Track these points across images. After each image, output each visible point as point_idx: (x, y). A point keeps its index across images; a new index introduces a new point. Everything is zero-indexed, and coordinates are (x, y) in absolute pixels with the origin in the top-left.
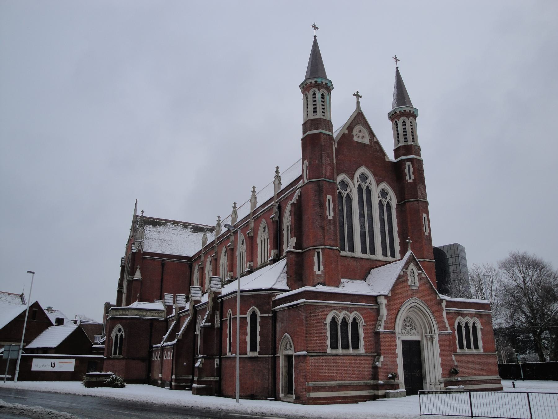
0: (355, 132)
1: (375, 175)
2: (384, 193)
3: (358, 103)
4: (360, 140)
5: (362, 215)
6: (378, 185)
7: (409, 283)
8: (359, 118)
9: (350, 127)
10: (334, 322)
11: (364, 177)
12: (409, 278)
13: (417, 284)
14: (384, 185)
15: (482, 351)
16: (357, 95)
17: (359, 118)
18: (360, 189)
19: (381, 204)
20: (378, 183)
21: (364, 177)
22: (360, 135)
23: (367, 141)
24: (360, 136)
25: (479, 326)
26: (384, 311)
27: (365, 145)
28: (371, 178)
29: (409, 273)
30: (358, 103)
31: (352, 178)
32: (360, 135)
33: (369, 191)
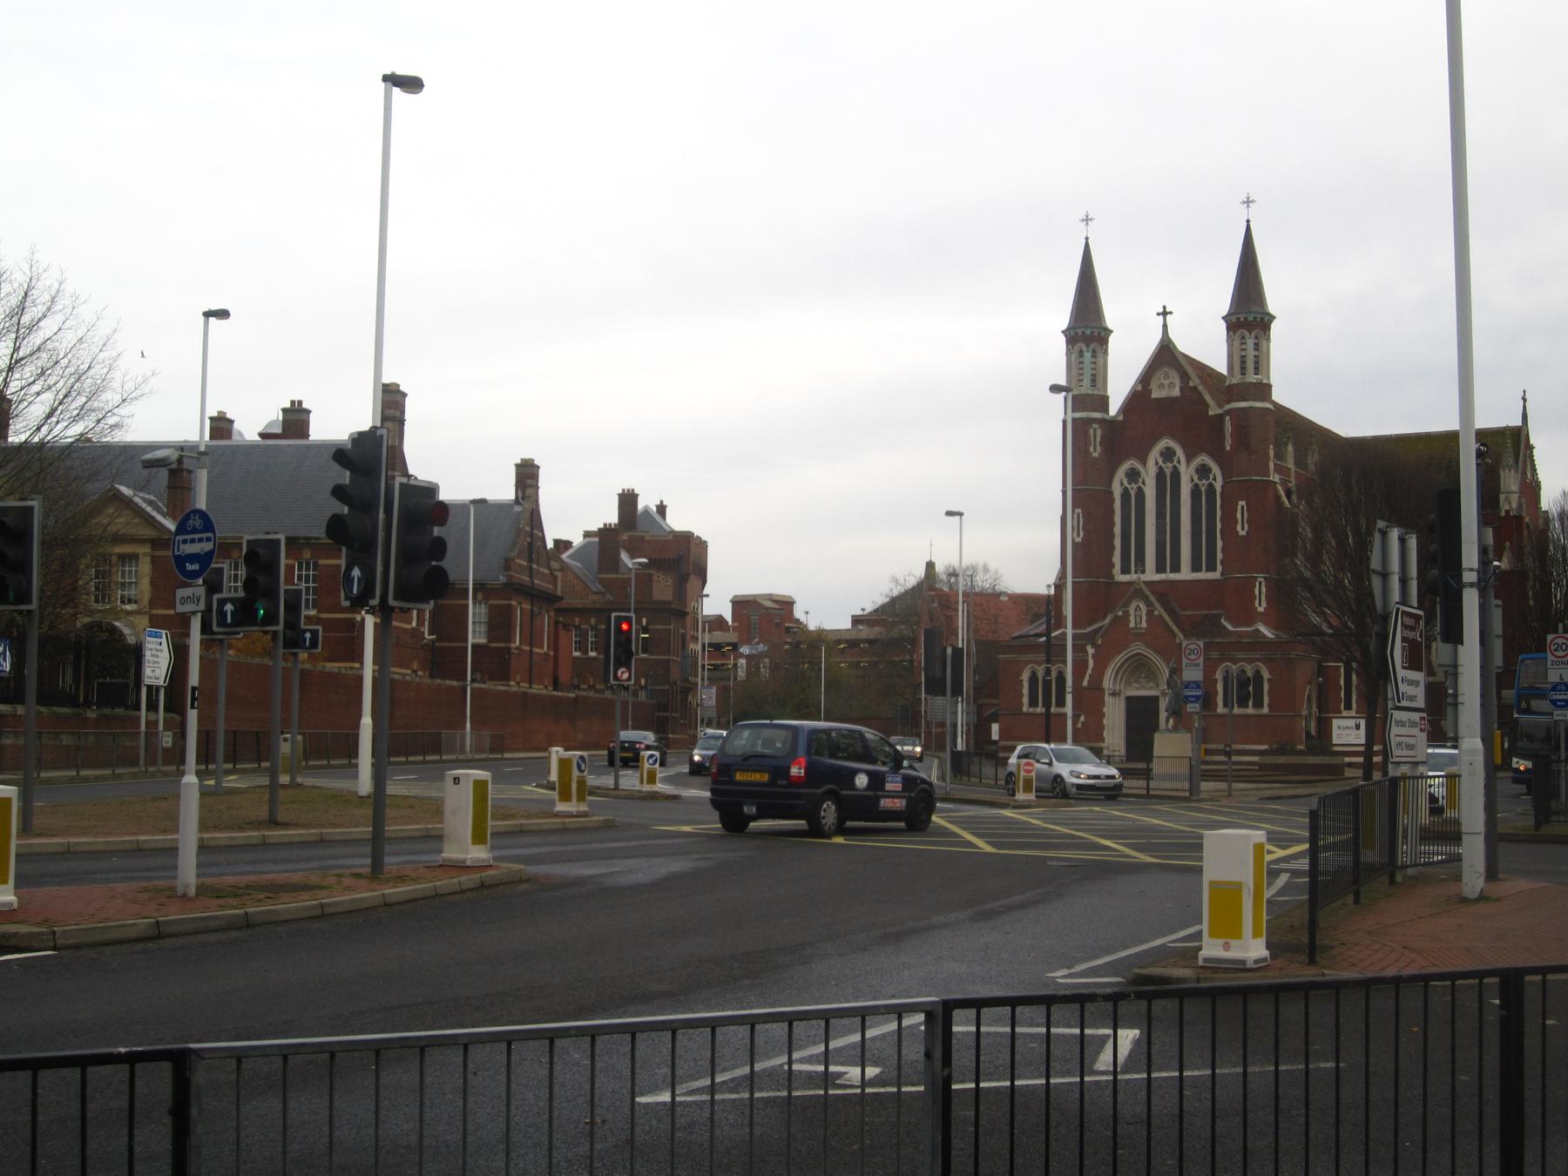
0: (1153, 385)
1: (1184, 447)
2: (1203, 471)
3: (1165, 326)
4: (1164, 394)
5: (1160, 515)
6: (1189, 460)
7: (1132, 625)
8: (1166, 354)
9: (1146, 378)
10: (1033, 679)
11: (1168, 454)
12: (1132, 618)
13: (1144, 625)
14: (1204, 459)
15: (1266, 710)
16: (1165, 313)
17: (1166, 354)
18: (1160, 475)
19: (1195, 493)
20: (1189, 460)
21: (1168, 454)
22: (1166, 382)
23: (1176, 392)
24: (1167, 388)
25: (1266, 675)
26: (1091, 663)
27: (1170, 400)
28: (1180, 453)
29: (1132, 612)
30: (1165, 326)
31: (1144, 463)
32: (1166, 382)
33: (1176, 475)
